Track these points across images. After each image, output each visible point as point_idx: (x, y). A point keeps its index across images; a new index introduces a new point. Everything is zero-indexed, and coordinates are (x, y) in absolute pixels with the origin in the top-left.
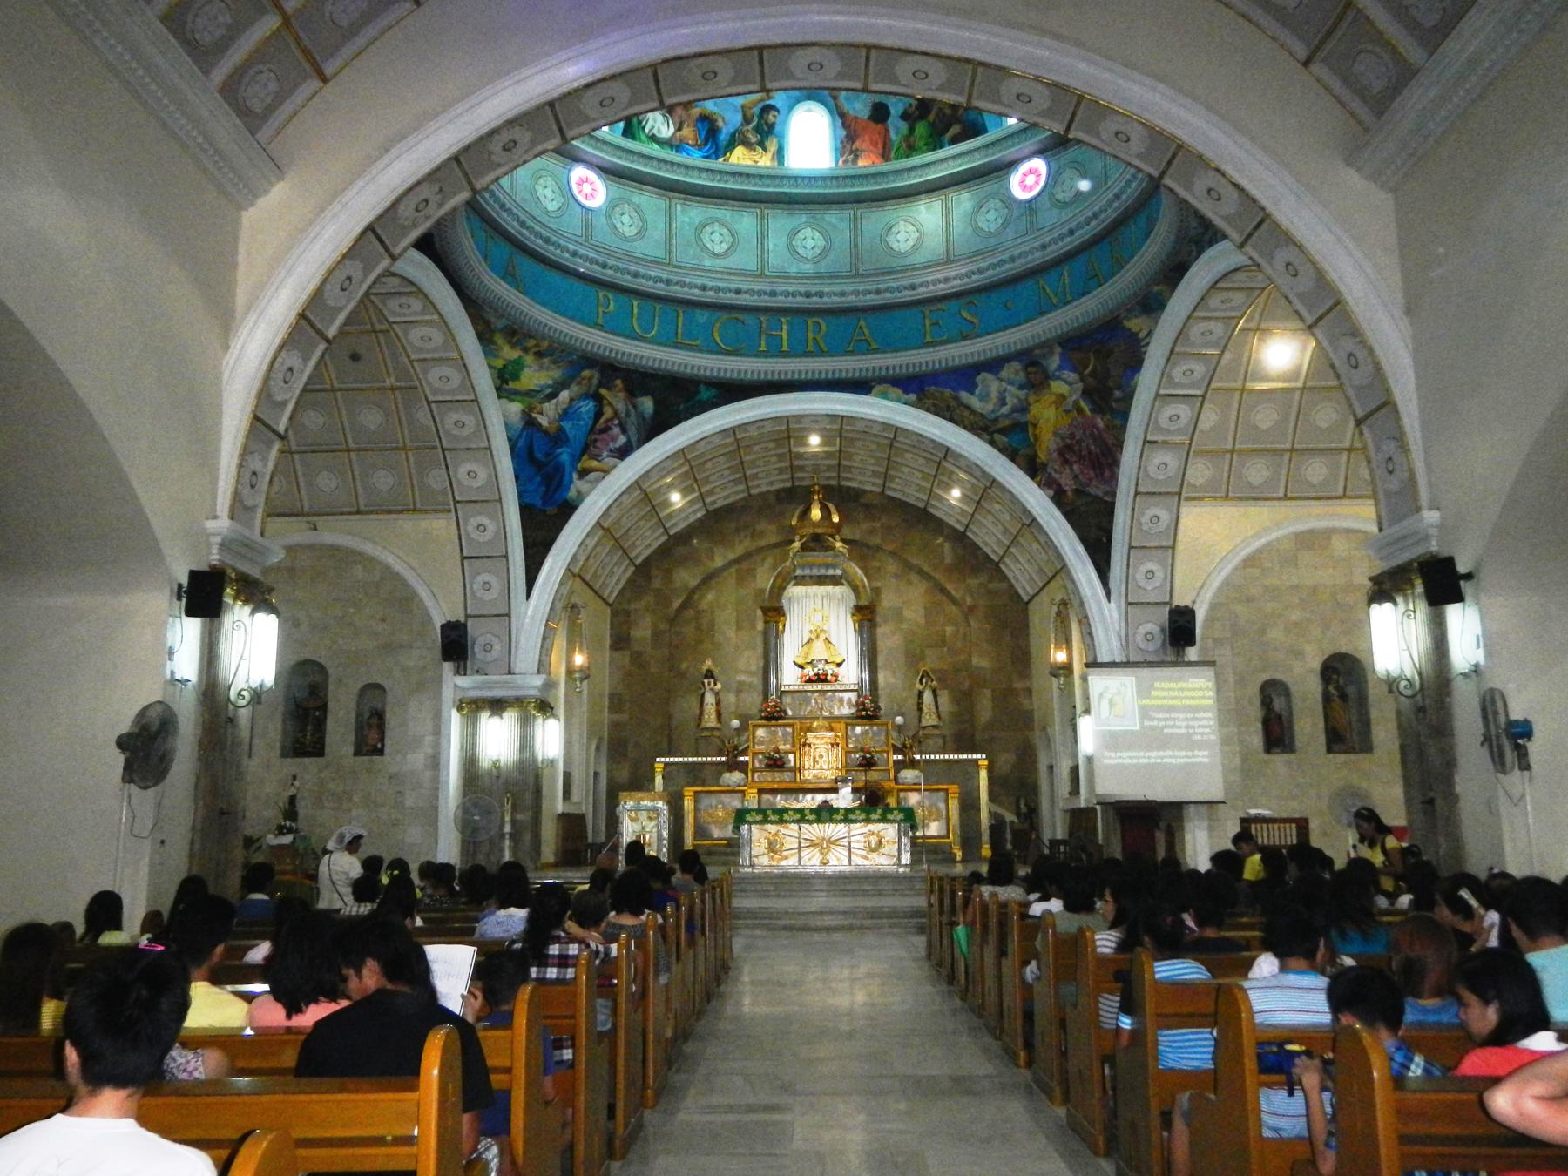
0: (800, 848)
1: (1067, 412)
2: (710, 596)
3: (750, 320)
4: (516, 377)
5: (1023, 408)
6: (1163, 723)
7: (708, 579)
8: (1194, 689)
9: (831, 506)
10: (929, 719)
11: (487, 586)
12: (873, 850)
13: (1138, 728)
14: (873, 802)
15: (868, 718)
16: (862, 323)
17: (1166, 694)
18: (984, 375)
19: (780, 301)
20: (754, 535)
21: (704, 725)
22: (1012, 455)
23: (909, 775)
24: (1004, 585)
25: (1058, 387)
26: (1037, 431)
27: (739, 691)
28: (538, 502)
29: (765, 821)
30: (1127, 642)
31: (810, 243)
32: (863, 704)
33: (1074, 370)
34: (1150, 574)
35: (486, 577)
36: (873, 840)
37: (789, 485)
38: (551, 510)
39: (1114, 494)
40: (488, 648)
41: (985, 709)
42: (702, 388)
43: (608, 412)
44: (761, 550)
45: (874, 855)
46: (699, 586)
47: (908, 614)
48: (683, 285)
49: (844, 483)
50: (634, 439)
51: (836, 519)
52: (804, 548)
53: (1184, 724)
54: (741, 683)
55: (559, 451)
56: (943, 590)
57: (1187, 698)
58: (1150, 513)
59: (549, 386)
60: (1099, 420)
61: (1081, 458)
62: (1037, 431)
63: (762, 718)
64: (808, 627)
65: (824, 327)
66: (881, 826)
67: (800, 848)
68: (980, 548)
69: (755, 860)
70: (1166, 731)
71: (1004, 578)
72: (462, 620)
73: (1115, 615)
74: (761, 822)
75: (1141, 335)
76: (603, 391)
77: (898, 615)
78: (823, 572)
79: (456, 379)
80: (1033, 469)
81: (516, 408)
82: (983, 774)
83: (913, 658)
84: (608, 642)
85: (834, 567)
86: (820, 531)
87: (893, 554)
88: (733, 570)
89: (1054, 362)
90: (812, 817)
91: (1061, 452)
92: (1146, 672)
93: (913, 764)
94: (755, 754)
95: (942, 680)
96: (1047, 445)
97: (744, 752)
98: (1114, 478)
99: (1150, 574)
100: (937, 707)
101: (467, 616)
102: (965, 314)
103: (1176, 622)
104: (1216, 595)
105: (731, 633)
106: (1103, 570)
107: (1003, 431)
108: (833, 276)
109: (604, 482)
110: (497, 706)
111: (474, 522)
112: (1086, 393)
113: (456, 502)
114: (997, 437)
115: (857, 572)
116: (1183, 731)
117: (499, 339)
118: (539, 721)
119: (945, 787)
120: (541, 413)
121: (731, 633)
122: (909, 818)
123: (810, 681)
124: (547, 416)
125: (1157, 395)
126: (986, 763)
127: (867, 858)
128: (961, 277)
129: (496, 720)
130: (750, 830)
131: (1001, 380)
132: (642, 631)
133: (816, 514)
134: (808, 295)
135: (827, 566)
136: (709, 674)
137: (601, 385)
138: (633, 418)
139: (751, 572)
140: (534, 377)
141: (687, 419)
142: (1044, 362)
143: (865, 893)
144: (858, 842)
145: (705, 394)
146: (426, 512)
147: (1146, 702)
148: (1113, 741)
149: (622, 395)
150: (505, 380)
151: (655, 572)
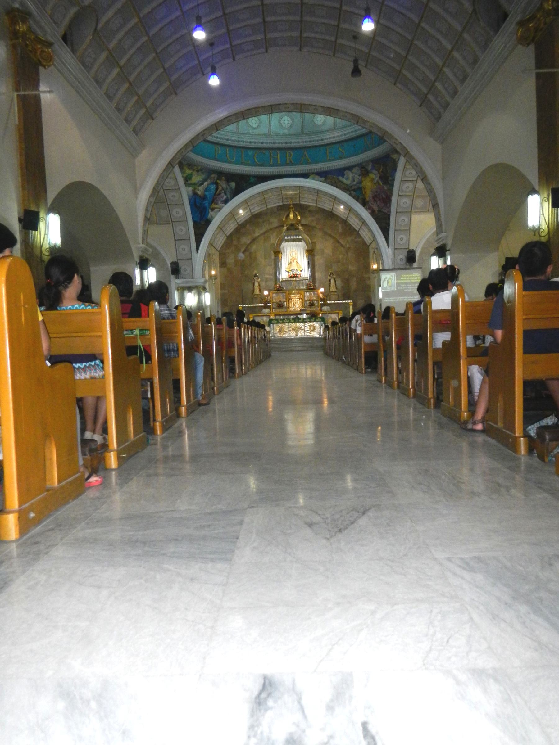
0: (289, 331)
1: (375, 184)
3: (267, 152)
4: (190, 179)
5: (360, 182)
6: (404, 288)
7: (254, 240)
8: (414, 277)
9: (297, 213)
10: (333, 289)
12: (312, 331)
13: (396, 289)
14: (313, 317)
15: (312, 289)
16: (305, 152)
17: (405, 278)
18: (347, 171)
21: (255, 293)
23: (325, 308)
24: (360, 240)
25: (372, 176)
27: (266, 281)
29: (278, 323)
30: (394, 262)
31: (286, 122)
32: (310, 284)
33: (376, 170)
35: (183, 246)
36: (312, 329)
37: (281, 204)
38: (203, 223)
39: (390, 212)
40: (185, 270)
41: (354, 285)
42: (251, 178)
43: (220, 188)
44: (271, 229)
45: (312, 332)
47: (326, 251)
48: (244, 142)
49: (302, 203)
50: (229, 197)
52: (287, 229)
53: (411, 288)
54: (267, 278)
55: (204, 202)
56: (339, 242)
57: (413, 280)
58: (402, 218)
59: (201, 181)
62: (366, 190)
63: (275, 290)
64: (290, 257)
65: (292, 153)
66: (314, 323)
67: (289, 331)
68: (352, 226)
69: (275, 335)
70: (405, 290)
71: (361, 237)
72: (176, 261)
73: (391, 253)
74: (276, 323)
75: (396, 160)
76: (218, 181)
77: (323, 252)
78: (295, 237)
79: (173, 182)
80: (364, 203)
81: (190, 189)
82: (351, 307)
83: (328, 266)
86: (294, 222)
89: (370, 168)
90: (292, 321)
91: (373, 198)
92: (399, 272)
94: (273, 303)
95: (337, 275)
96: (369, 195)
97: (269, 303)
98: (390, 206)
100: (336, 285)
101: (178, 259)
102: (340, 149)
103: (409, 255)
106: (387, 237)
107: (354, 190)
108: (295, 135)
109: (220, 213)
110: (190, 289)
111: (178, 228)
112: (381, 178)
113: (172, 222)
114: (352, 192)
116: (410, 290)
117: (185, 168)
118: (203, 294)
119: (338, 312)
120: (198, 190)
122: (323, 320)
124: (200, 191)
126: (352, 303)
127: (310, 333)
128: (338, 136)
129: (190, 294)
130: (273, 326)
131: (353, 173)
132: (230, 261)
133: (292, 216)
134: (286, 143)
135: (296, 236)
136: (256, 276)
137: (218, 179)
138: (229, 190)
139: (269, 238)
140: (196, 178)
141: (247, 189)
142: (366, 167)
144: (307, 328)
145: (252, 180)
146: (160, 224)
147: (399, 281)
148: (385, 294)
149: (224, 182)
150: (187, 179)
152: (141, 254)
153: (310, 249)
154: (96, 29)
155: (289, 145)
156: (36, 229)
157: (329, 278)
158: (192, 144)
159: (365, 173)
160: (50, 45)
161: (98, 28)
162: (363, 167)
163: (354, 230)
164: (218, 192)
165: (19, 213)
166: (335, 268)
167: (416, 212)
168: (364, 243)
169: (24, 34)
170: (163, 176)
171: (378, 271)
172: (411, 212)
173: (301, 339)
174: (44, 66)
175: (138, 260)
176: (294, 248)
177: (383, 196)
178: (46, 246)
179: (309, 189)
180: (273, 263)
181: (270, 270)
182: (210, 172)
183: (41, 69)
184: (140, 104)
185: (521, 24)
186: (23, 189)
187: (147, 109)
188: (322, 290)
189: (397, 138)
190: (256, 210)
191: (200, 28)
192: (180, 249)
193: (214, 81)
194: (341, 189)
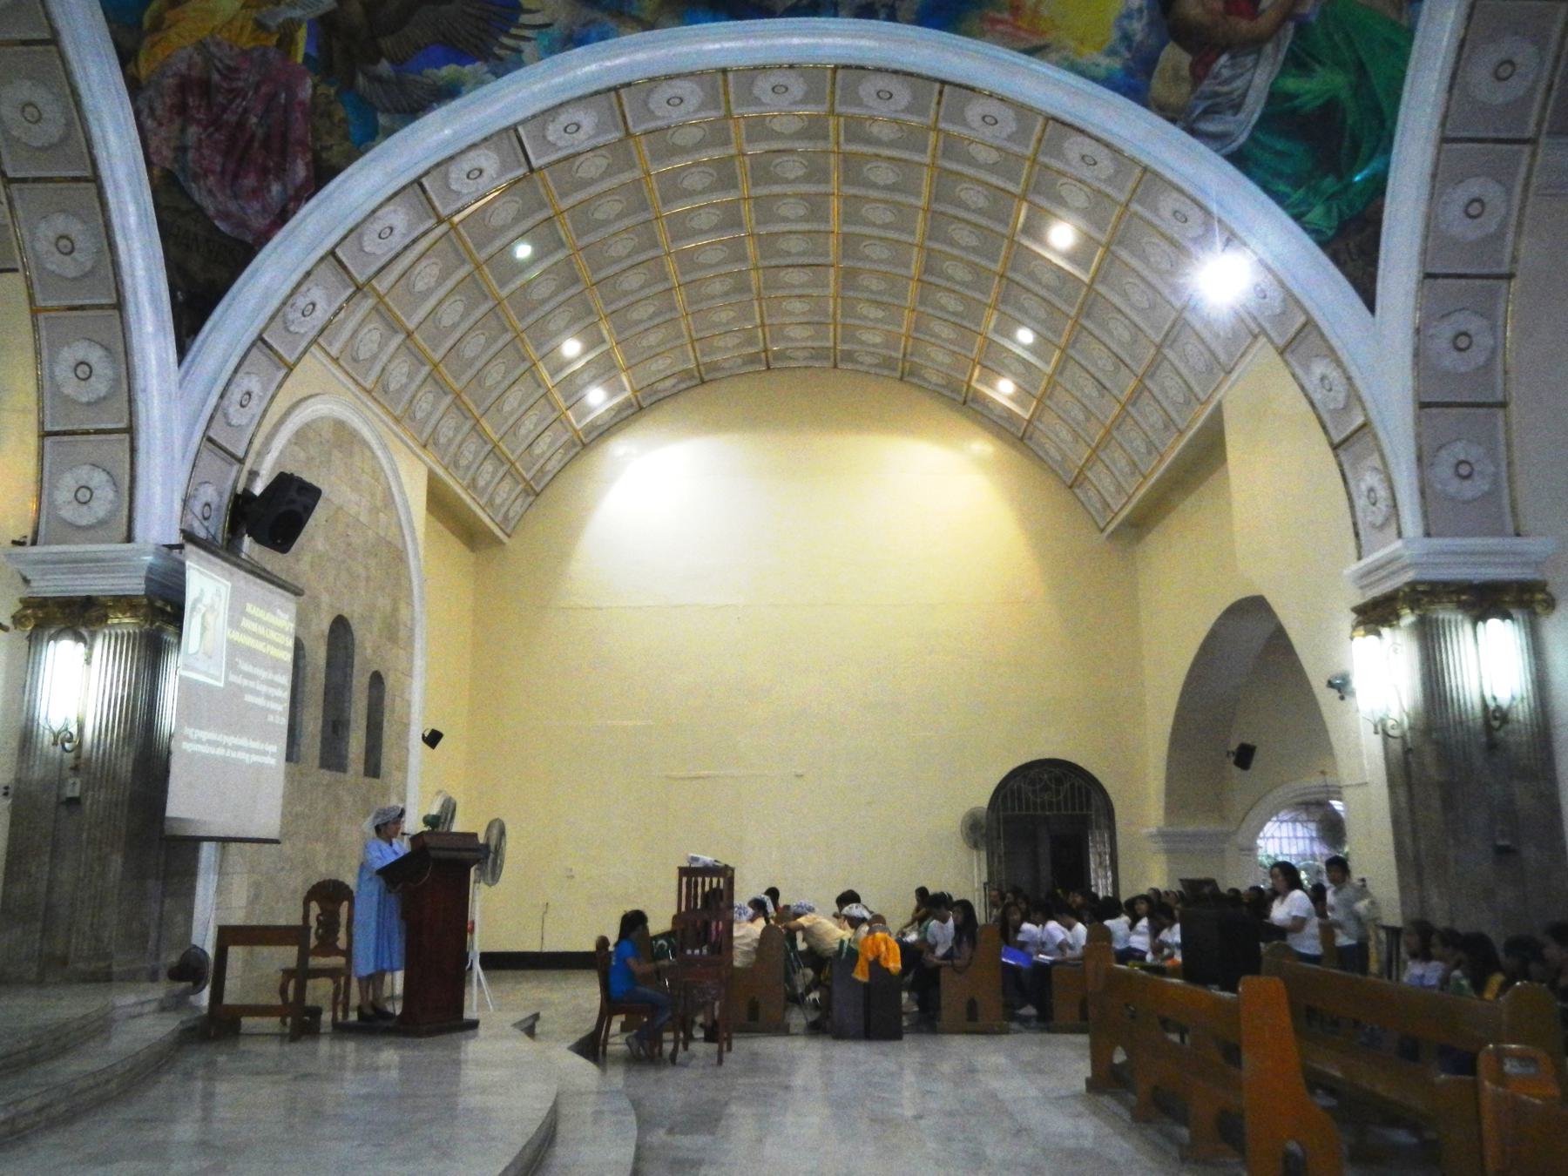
1: (260, 26)
26: (170, 16)
60: (309, 82)
61: (215, 123)
62: (170, 16)
70: (249, 698)
75: (525, 19)
91: (185, 85)
177: (254, 120)
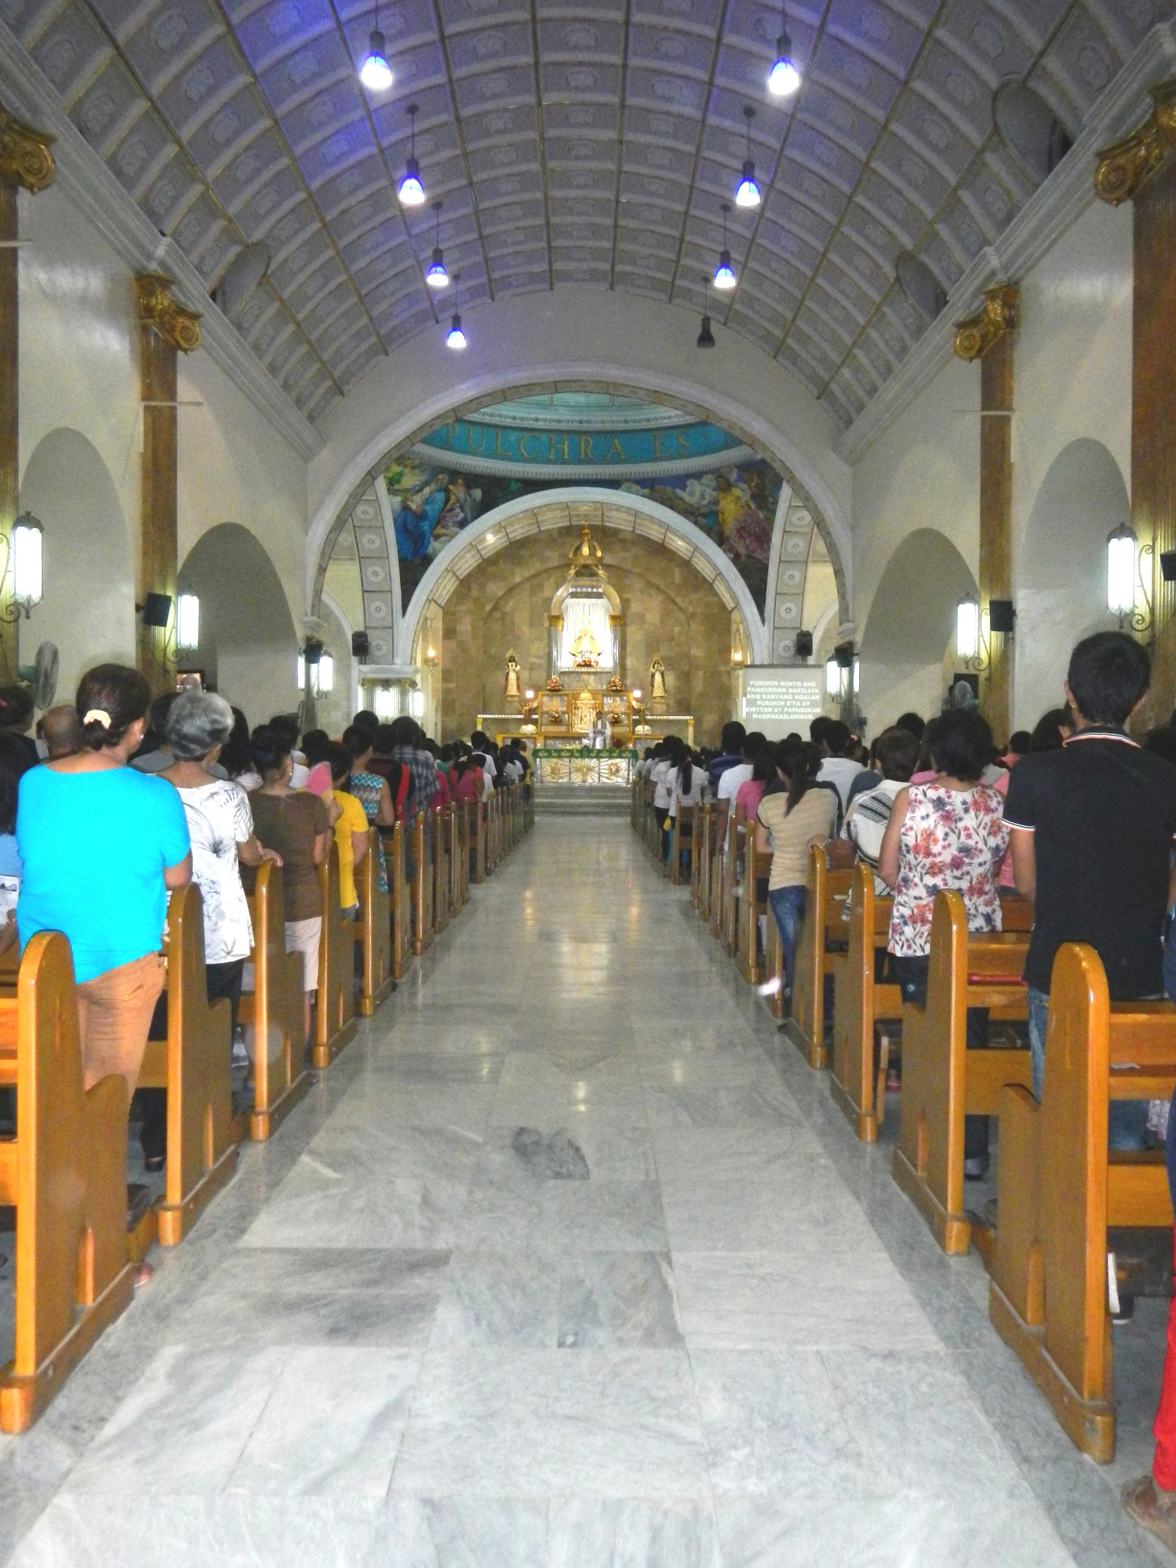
0: (570, 773)
2: (511, 603)
3: (544, 438)
4: (398, 482)
5: (716, 503)
7: (511, 590)
10: (658, 691)
11: (378, 609)
14: (617, 746)
16: (616, 441)
18: (692, 481)
19: (563, 426)
20: (543, 559)
22: (708, 531)
24: (716, 599)
25: (736, 492)
28: (410, 557)
29: (550, 756)
33: (745, 482)
34: (789, 610)
37: (567, 524)
38: (418, 561)
40: (379, 648)
41: (698, 684)
42: (513, 483)
43: (453, 499)
44: (546, 571)
46: (503, 596)
49: (609, 524)
50: (469, 516)
51: (599, 554)
52: (577, 574)
56: (673, 601)
58: (788, 573)
61: (751, 535)
66: (618, 760)
67: (570, 773)
71: (716, 594)
73: (767, 634)
76: (451, 487)
77: (641, 618)
80: (721, 540)
81: (398, 499)
82: (691, 730)
83: (651, 647)
84: (441, 633)
85: (598, 588)
86: (589, 562)
87: (640, 575)
88: (528, 585)
89: (733, 477)
90: (577, 754)
91: (738, 531)
93: (647, 722)
94: (543, 713)
95: (670, 663)
96: (730, 526)
98: (769, 548)
99: (789, 610)
101: (366, 627)
104: (828, 624)
105: (525, 628)
106: (761, 605)
107: (703, 515)
110: (386, 684)
112: (753, 497)
114: (699, 518)
115: (612, 592)
121: (525, 628)
123: (579, 665)
124: (415, 503)
125: (790, 506)
129: (385, 693)
132: (465, 626)
133: (585, 550)
135: (593, 587)
136: (512, 659)
139: (541, 586)
140: (410, 480)
143: (607, 797)
145: (514, 486)
151: (473, 585)
152: (309, 632)
153: (617, 613)
154: (265, 274)
155: (585, 427)
156: (163, 623)
157: (652, 670)
158: (410, 439)
159: (724, 486)
160: (195, 317)
161: (270, 271)
162: (721, 476)
163: (705, 580)
164: (448, 507)
165: (137, 596)
166: (665, 650)
167: (816, 562)
168: (723, 606)
169: (163, 313)
170: (356, 497)
171: (742, 665)
172: (807, 562)
173: (592, 791)
174: (185, 351)
175: (302, 645)
176: (587, 608)
178: (172, 647)
179: (619, 508)
180: (545, 635)
181: (538, 648)
182: (435, 470)
183: (180, 354)
184: (325, 371)
185: (962, 326)
186: (145, 554)
187: (334, 381)
188: (637, 694)
189: (775, 451)
190: (518, 532)
191: (439, 269)
192: (373, 609)
193: (457, 341)
194: (679, 512)
